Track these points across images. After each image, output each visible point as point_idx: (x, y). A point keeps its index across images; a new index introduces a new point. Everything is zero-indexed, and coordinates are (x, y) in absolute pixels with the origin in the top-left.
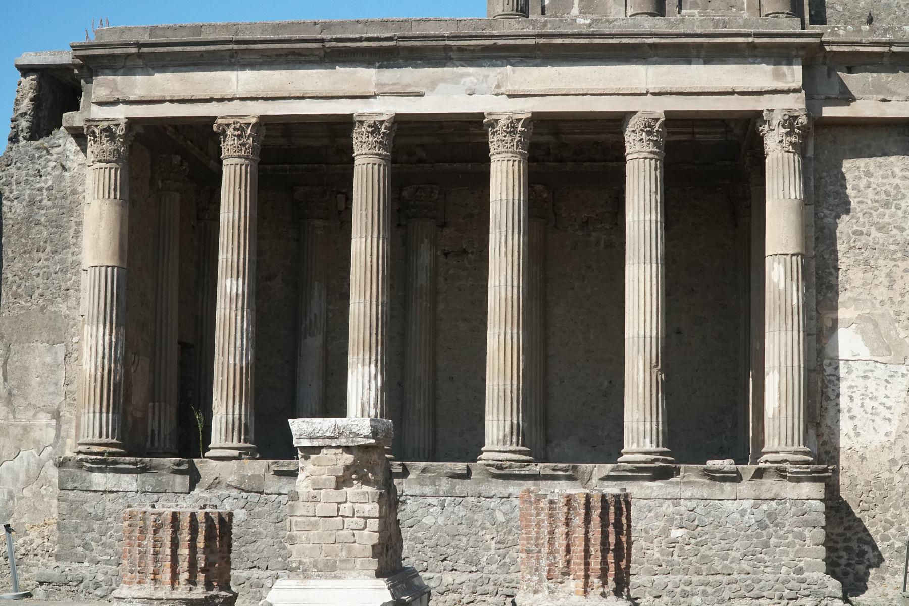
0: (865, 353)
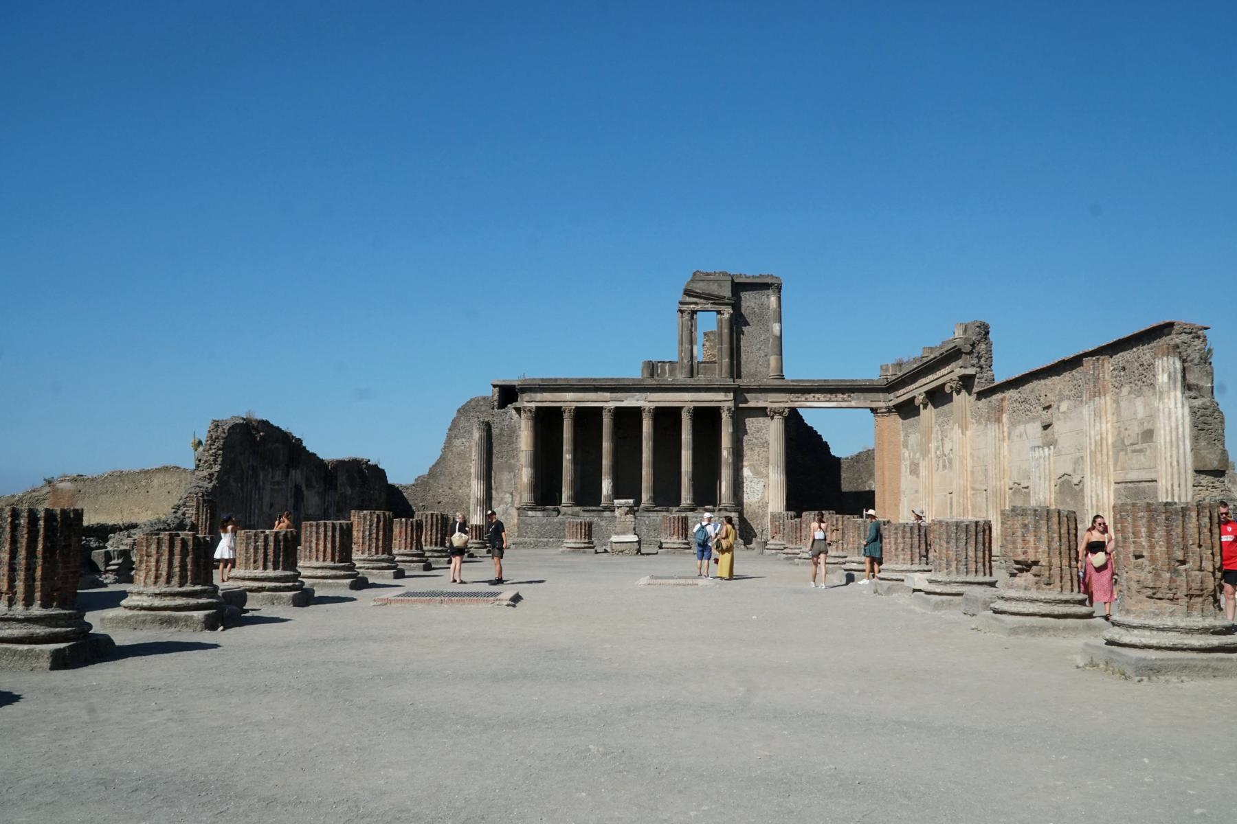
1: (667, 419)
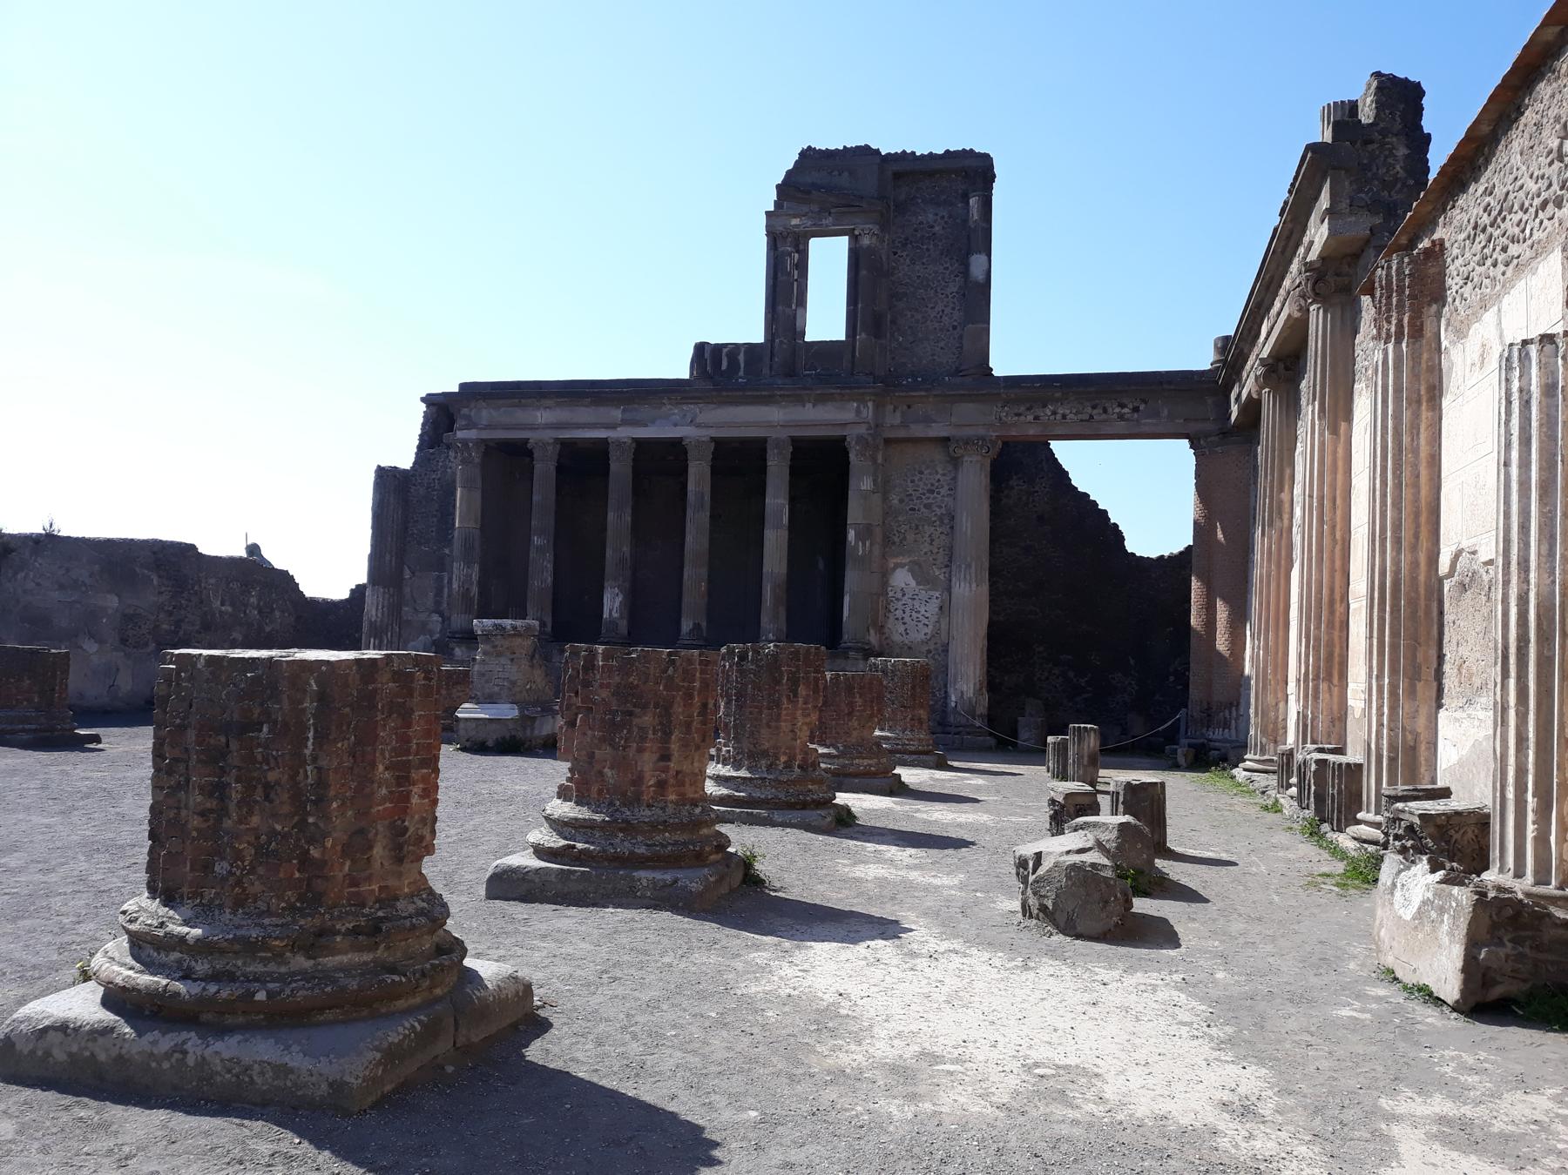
0: (913, 583)
1: (739, 462)
